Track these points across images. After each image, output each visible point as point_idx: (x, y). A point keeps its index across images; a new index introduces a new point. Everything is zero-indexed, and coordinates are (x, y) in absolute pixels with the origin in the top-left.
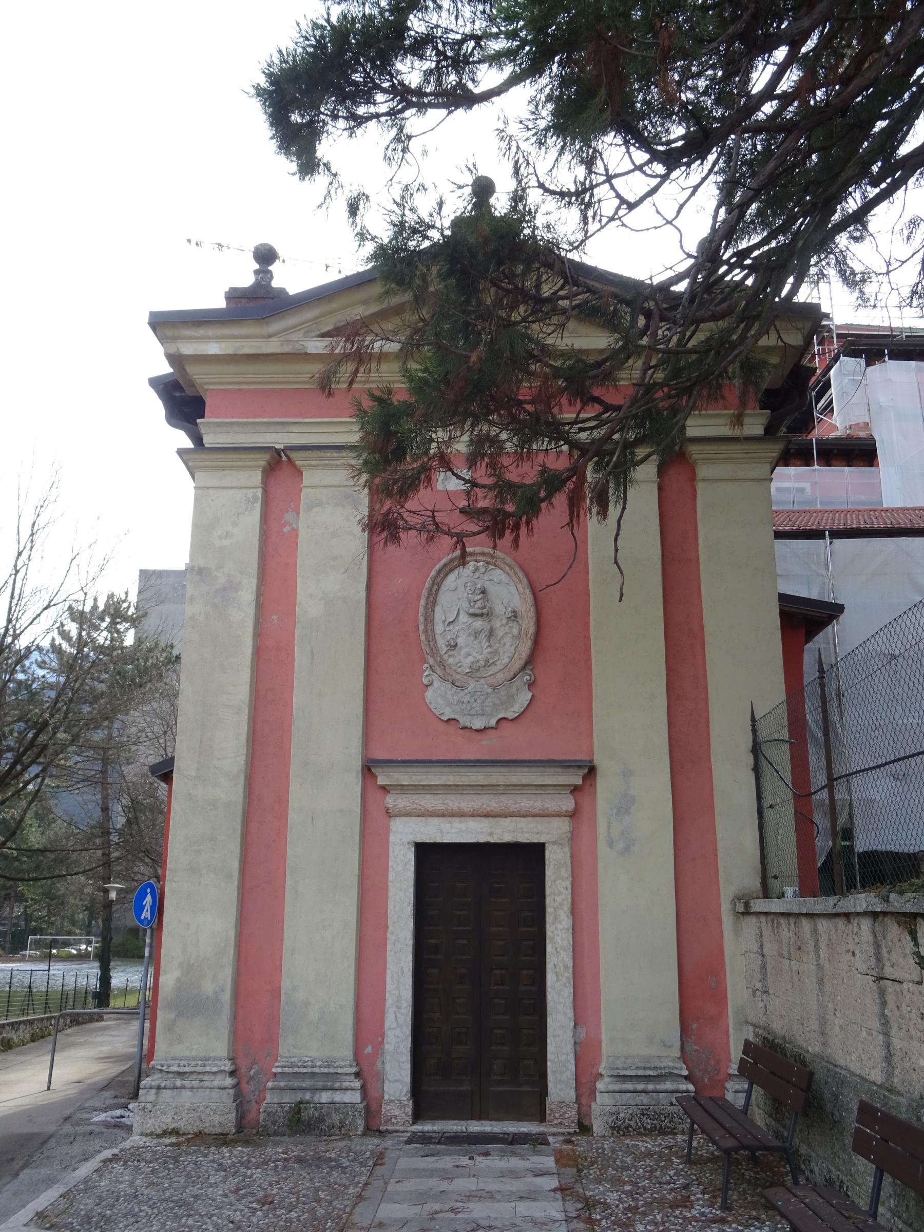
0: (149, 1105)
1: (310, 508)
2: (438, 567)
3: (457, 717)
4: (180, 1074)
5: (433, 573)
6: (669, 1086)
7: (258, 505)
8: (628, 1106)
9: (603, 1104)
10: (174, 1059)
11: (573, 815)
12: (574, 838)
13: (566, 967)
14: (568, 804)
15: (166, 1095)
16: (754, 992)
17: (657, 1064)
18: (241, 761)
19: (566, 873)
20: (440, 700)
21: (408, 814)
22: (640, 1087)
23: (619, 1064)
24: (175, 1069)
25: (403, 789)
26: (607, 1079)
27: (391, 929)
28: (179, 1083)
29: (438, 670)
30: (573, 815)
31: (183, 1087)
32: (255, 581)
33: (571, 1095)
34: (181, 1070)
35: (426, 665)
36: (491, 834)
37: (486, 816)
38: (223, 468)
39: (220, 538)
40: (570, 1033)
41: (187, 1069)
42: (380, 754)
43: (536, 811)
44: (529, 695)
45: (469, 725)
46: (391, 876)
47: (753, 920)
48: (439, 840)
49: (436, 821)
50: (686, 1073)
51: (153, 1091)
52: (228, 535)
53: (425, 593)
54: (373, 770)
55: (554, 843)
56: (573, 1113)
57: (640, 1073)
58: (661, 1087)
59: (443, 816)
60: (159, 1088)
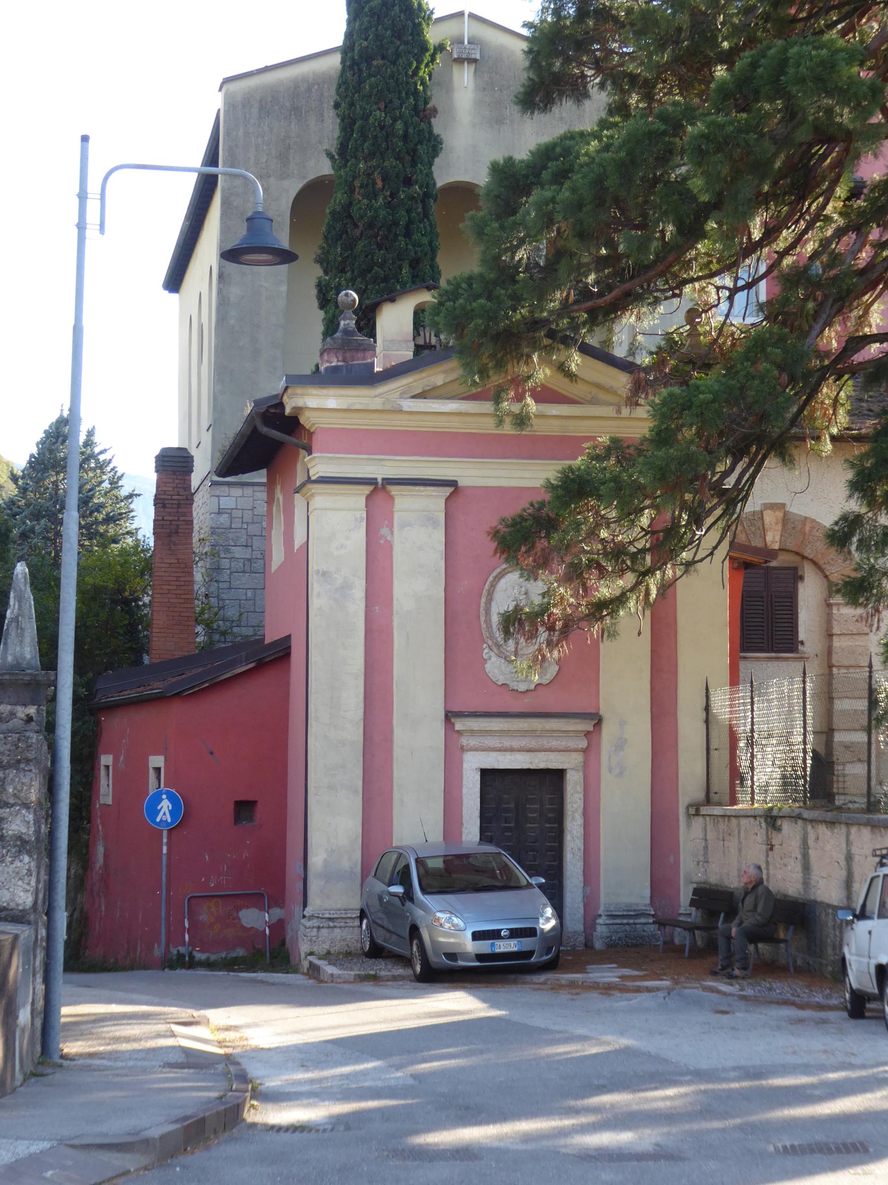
0: (314, 938)
1: (403, 526)
2: (494, 574)
3: (508, 682)
4: (330, 919)
5: (491, 579)
6: (643, 920)
7: (364, 524)
8: (617, 933)
9: (601, 930)
10: (326, 910)
11: (585, 751)
12: (586, 766)
13: (579, 849)
14: (583, 744)
15: (324, 932)
16: (698, 863)
17: (635, 908)
18: (361, 713)
19: (580, 789)
20: (496, 671)
21: (476, 750)
22: (625, 921)
23: (612, 908)
24: (327, 916)
25: (472, 732)
26: (604, 917)
27: (465, 825)
28: (331, 924)
29: (495, 649)
30: (585, 751)
31: (335, 927)
32: (364, 582)
33: (580, 927)
34: (332, 916)
35: (485, 646)
36: (531, 763)
37: (528, 751)
38: (337, 495)
39: (337, 548)
40: (581, 890)
41: (335, 916)
42: (456, 708)
43: (562, 748)
44: (557, 668)
45: (516, 688)
46: (465, 791)
47: (701, 819)
48: (497, 767)
49: (494, 754)
50: (653, 913)
51: (315, 930)
52: (342, 546)
53: (485, 592)
54: (453, 720)
55: (573, 769)
56: (582, 939)
57: (625, 913)
58: (638, 921)
59: (500, 751)
60: (319, 928)
